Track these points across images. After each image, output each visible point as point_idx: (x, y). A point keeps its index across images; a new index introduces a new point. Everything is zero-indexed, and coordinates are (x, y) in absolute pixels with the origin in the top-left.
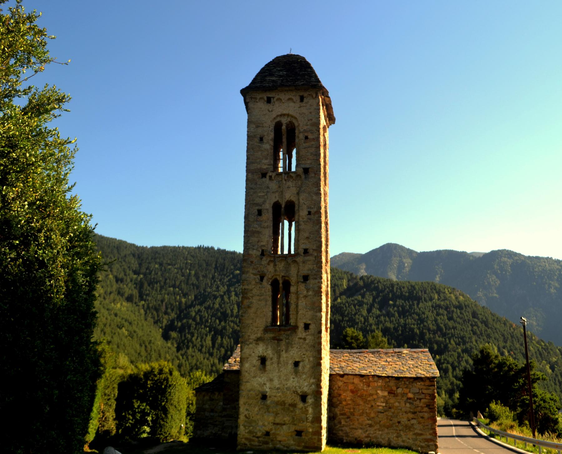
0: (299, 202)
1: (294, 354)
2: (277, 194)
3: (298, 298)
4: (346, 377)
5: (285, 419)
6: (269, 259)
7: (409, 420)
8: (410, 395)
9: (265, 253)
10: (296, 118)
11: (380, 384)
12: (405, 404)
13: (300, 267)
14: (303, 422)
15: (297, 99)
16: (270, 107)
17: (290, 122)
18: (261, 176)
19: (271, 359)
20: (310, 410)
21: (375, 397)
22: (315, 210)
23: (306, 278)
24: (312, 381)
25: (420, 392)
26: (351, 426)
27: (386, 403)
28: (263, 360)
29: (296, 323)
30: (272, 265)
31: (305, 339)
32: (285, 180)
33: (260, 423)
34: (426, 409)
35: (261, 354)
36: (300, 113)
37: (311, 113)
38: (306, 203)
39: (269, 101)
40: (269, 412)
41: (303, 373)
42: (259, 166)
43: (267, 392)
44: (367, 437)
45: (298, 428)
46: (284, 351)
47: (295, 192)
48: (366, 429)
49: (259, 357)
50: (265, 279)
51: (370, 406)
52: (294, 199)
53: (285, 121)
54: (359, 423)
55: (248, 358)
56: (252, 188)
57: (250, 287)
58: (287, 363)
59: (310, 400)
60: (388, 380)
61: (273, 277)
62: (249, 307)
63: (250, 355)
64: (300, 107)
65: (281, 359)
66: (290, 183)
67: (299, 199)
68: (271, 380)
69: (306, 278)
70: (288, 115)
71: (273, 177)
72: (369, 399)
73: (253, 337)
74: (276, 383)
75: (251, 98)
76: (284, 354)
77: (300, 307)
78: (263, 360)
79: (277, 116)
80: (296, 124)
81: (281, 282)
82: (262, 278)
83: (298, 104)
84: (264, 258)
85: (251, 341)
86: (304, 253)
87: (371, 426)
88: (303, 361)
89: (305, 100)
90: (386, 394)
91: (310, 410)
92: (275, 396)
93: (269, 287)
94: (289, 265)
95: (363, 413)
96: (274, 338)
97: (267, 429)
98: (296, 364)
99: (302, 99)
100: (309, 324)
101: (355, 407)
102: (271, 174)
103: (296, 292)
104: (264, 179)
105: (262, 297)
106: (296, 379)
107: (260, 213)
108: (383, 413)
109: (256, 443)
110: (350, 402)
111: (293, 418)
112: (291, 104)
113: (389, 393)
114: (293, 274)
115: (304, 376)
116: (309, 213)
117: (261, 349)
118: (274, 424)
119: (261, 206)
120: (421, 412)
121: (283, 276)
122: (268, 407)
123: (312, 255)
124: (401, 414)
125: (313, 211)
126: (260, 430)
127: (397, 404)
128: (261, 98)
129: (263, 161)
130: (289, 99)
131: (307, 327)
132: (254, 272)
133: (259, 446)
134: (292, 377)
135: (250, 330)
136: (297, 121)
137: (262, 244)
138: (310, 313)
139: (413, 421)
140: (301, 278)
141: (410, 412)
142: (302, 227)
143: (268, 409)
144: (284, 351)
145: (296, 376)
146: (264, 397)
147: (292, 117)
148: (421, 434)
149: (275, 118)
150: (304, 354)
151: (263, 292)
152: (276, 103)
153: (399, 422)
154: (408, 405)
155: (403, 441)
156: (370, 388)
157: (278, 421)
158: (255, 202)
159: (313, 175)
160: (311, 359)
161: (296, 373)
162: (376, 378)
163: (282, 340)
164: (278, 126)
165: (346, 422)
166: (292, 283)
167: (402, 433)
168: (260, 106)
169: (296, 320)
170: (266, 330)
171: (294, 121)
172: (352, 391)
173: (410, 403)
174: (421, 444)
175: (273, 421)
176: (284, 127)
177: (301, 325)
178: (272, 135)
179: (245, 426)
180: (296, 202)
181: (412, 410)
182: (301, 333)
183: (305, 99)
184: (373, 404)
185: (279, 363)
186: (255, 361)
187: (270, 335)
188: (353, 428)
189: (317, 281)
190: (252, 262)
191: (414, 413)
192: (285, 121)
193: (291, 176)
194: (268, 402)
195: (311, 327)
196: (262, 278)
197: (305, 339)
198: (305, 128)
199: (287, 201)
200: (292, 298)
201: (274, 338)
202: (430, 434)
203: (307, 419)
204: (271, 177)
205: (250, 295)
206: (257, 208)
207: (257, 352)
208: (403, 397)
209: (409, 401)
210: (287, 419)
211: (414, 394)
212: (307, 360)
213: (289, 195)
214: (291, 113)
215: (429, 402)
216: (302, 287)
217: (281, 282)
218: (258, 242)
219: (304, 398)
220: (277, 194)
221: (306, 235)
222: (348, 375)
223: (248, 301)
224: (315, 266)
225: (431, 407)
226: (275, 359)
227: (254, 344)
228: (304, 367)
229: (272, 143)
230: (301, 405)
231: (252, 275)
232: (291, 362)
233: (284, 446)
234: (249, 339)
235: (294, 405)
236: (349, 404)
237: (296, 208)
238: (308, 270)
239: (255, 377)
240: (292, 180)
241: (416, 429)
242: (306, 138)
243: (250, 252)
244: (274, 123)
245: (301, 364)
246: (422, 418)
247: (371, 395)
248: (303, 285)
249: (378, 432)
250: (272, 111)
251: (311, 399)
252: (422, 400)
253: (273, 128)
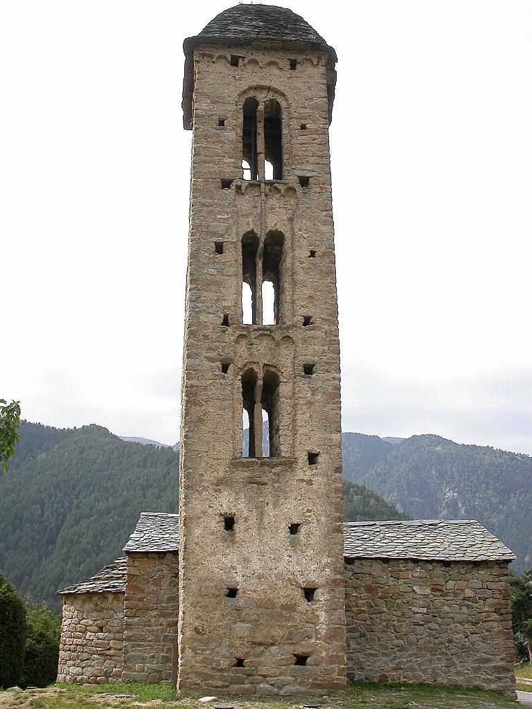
0: (293, 234)
1: (291, 509)
2: (250, 220)
3: (295, 406)
4: (357, 563)
5: (274, 633)
6: (238, 333)
7: (467, 637)
8: (469, 593)
9: (230, 321)
10: (284, 95)
11: (417, 575)
12: (460, 609)
13: (298, 349)
14: (310, 638)
15: (285, 64)
16: (238, 72)
17: (271, 100)
18: (220, 185)
19: (246, 520)
20: (323, 617)
21: (409, 597)
22: (323, 249)
23: (309, 369)
24: (325, 560)
25: (485, 587)
26: (368, 651)
27: (428, 608)
28: (229, 523)
29: (293, 452)
30: (244, 343)
31: (310, 482)
32: (266, 196)
33: (226, 642)
34: (496, 616)
35: (225, 509)
36: (290, 88)
37: (309, 88)
38: (305, 236)
39: (234, 62)
40: (243, 621)
41: (307, 545)
42: (217, 168)
43: (238, 582)
44: (395, 669)
45: (300, 650)
46: (270, 506)
47: (285, 218)
48: (394, 655)
49: (221, 515)
50: (231, 367)
51: (399, 614)
52: (284, 228)
53: (262, 97)
54: (381, 645)
55: (199, 518)
56: (204, 205)
57: (202, 383)
58: (278, 528)
59: (322, 596)
60: (430, 567)
61: (245, 366)
62: (201, 420)
63: (204, 513)
65: (266, 520)
66: (273, 201)
67: (292, 229)
68: (246, 560)
69: (309, 369)
70: (269, 89)
71: (243, 188)
72: (398, 601)
73: (210, 477)
74: (256, 565)
75: (203, 55)
76: (270, 511)
77: (299, 423)
78: (229, 523)
79: (250, 88)
80: (283, 104)
81: (261, 375)
82: (225, 368)
83: (288, 72)
84: (230, 329)
85: (206, 484)
86: (305, 324)
87: (401, 648)
88: (307, 523)
89: (298, 66)
90: (428, 591)
91: (323, 617)
92: (255, 591)
93: (239, 384)
94: (278, 344)
95: (388, 626)
96: (252, 481)
97: (239, 655)
98: (294, 529)
99: (293, 65)
100: (317, 455)
101: (371, 616)
102: (239, 183)
103: (290, 394)
104: (226, 191)
105: (226, 403)
106: (294, 558)
107: (219, 248)
108: (422, 625)
109: (220, 683)
110: (364, 608)
111: (291, 633)
112: (275, 71)
113: (433, 590)
114: (286, 362)
115: (310, 552)
116: (313, 254)
117: (226, 502)
118: (254, 643)
119: (221, 236)
120: (486, 621)
121: (265, 365)
122: (238, 610)
123: (319, 328)
124: (453, 626)
125: (320, 250)
126: (224, 656)
127: (446, 608)
128: (220, 57)
129: (226, 161)
130: (271, 63)
131: (312, 458)
132: (207, 355)
133: (224, 686)
134: (286, 553)
135: (203, 464)
137: (225, 304)
138: (318, 435)
139: (474, 638)
140: (301, 368)
141: (469, 622)
142: (300, 277)
143: (239, 616)
144: (270, 506)
145: (295, 551)
146: (232, 593)
147: (276, 91)
148: (488, 660)
149: (244, 92)
150: (309, 511)
151: (227, 392)
152: (249, 68)
153: (450, 641)
154: (465, 609)
155: (458, 673)
156: (401, 582)
157: (259, 637)
158: (211, 229)
159: (318, 190)
160: (323, 519)
161: (294, 545)
162: (410, 565)
163: (265, 484)
164: (250, 108)
165: (359, 644)
166: (282, 379)
167: (455, 659)
168: (216, 74)
169: (293, 446)
170: (235, 464)
172: (369, 589)
173: (468, 607)
174: (488, 677)
175: (250, 639)
176: (261, 107)
177: (303, 457)
178: (241, 119)
179: (194, 650)
180: (288, 235)
181: (470, 619)
182: (303, 470)
183: (298, 65)
184: (405, 611)
185: (261, 526)
186: (217, 525)
187: (242, 474)
188: (373, 655)
189: (330, 375)
190: (206, 337)
191: (475, 624)
192: (262, 97)
193: (276, 188)
194: (240, 601)
195: (320, 459)
196: (225, 368)
197: (310, 482)
199: (270, 231)
200: (284, 405)
201: (252, 481)
202: (502, 659)
203: (317, 632)
204: (239, 188)
205: (201, 397)
206: (214, 239)
207: (216, 505)
208: (456, 595)
209: (466, 602)
210: (278, 633)
211: (474, 589)
212: (315, 521)
213: (277, 221)
214: (274, 85)
215: (500, 604)
216: (303, 384)
217: (261, 375)
218: (218, 300)
219: (309, 593)
220: (250, 220)
221: (307, 292)
222: (359, 558)
223: (198, 409)
224: (326, 348)
225: (503, 611)
226: (253, 520)
227: (211, 492)
228: (308, 535)
229: (240, 131)
230: (303, 605)
231: (206, 362)
232: (284, 526)
233: (272, 685)
234: (202, 481)
235: (291, 608)
236: (364, 612)
237: (288, 244)
238: (315, 354)
239: (214, 554)
240: (278, 196)
241: (478, 651)
242: (303, 127)
243: (203, 318)
244: (244, 100)
245: (303, 530)
246: (488, 631)
247: (401, 595)
248: (307, 380)
249: (414, 660)
250: (240, 79)
251: (323, 594)
252: (489, 601)
253: (241, 107)
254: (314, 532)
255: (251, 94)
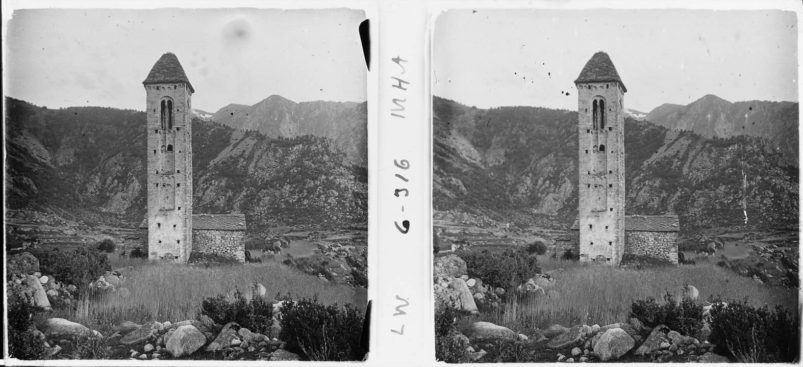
15: (605, 86)
35: (590, 223)
41: (610, 232)
53: (598, 99)
64: (606, 92)
70: (600, 96)
82: (589, 187)
115: (610, 233)
136: (605, 100)
147: (602, 97)
171: (603, 100)
180: (605, 146)
196: (589, 187)
198: (610, 104)
228: (610, 229)
245: (608, 228)
254: (611, 228)
255: (595, 99)
